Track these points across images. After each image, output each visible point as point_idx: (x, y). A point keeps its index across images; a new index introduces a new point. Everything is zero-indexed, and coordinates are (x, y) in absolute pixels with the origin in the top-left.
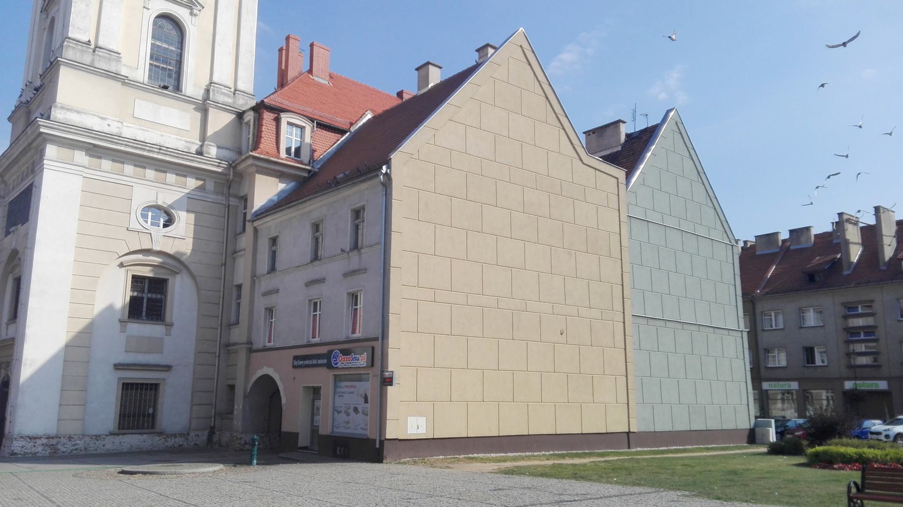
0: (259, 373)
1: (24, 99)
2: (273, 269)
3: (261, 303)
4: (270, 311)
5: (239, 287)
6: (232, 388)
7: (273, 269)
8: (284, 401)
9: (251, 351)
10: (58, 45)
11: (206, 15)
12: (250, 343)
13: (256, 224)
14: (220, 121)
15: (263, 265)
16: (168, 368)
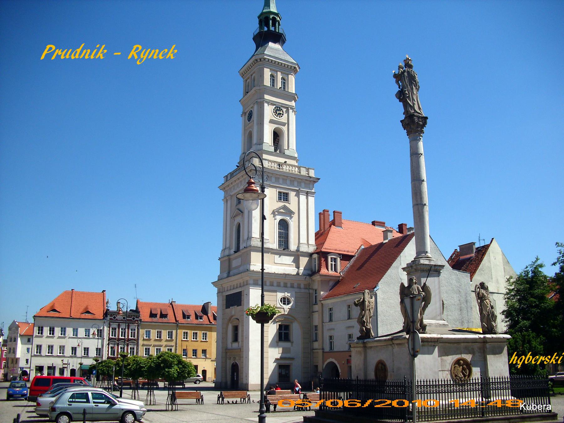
0: (328, 361)
1: (227, 252)
2: (331, 320)
3: (327, 335)
4: (331, 337)
5: (316, 326)
6: (317, 366)
7: (331, 320)
8: (340, 371)
9: (323, 352)
10: (246, 237)
11: (295, 216)
12: (323, 349)
13: (322, 302)
14: (304, 261)
15: (327, 318)
16: (292, 359)
